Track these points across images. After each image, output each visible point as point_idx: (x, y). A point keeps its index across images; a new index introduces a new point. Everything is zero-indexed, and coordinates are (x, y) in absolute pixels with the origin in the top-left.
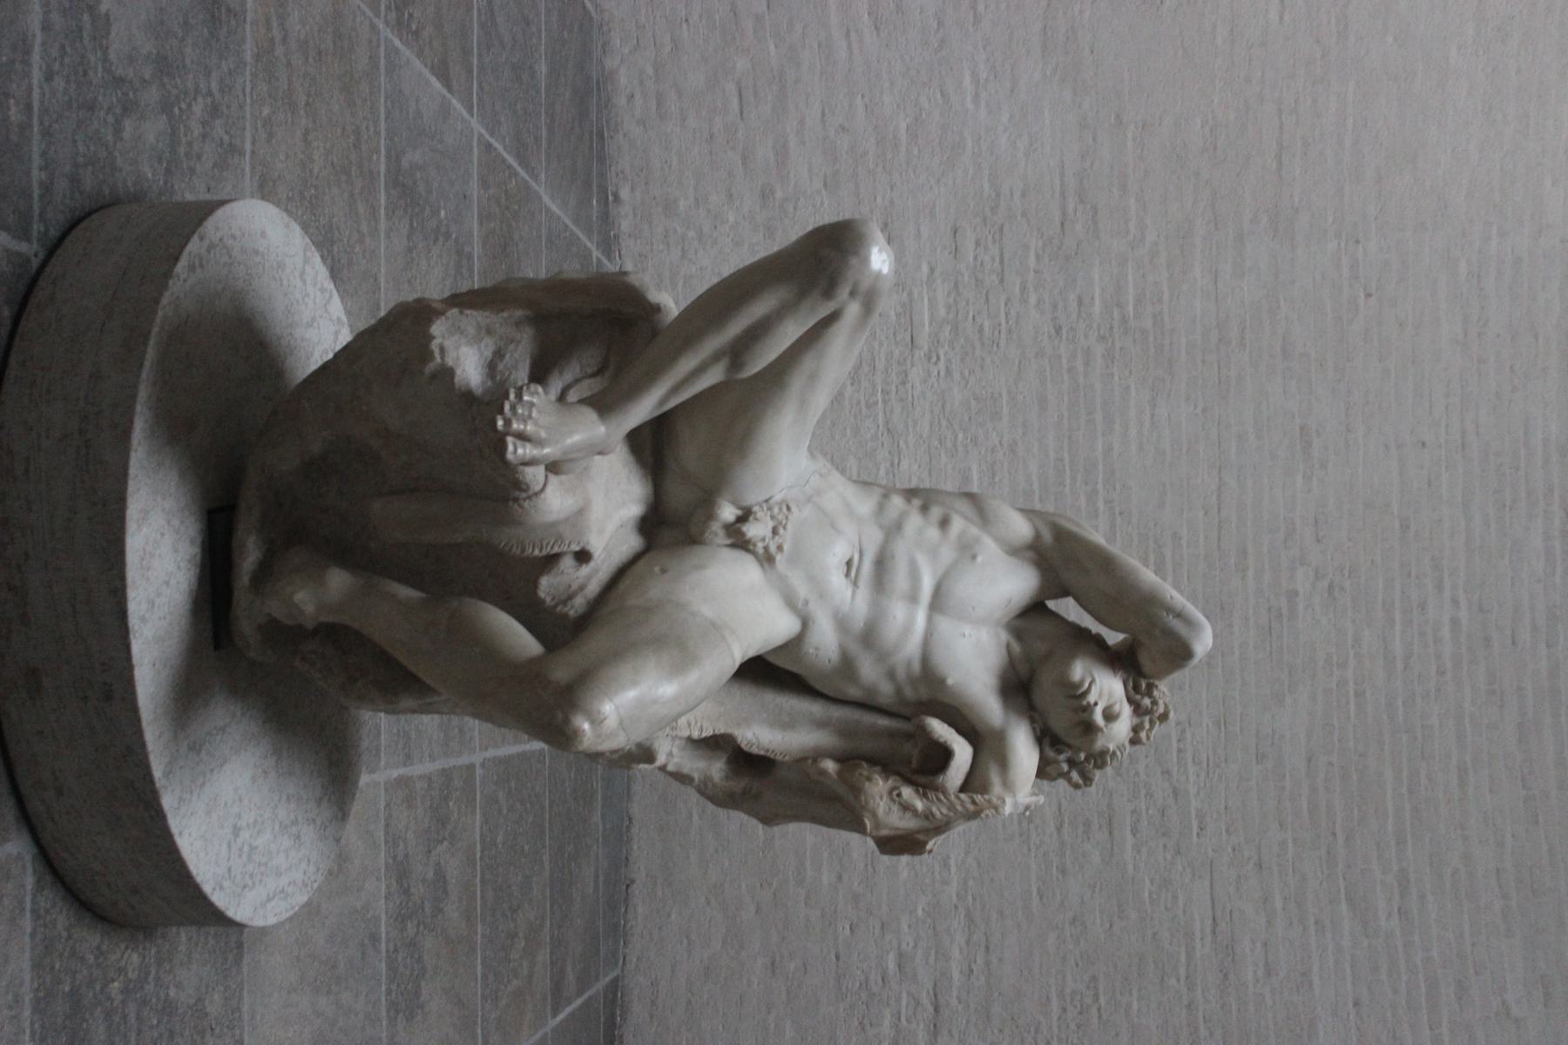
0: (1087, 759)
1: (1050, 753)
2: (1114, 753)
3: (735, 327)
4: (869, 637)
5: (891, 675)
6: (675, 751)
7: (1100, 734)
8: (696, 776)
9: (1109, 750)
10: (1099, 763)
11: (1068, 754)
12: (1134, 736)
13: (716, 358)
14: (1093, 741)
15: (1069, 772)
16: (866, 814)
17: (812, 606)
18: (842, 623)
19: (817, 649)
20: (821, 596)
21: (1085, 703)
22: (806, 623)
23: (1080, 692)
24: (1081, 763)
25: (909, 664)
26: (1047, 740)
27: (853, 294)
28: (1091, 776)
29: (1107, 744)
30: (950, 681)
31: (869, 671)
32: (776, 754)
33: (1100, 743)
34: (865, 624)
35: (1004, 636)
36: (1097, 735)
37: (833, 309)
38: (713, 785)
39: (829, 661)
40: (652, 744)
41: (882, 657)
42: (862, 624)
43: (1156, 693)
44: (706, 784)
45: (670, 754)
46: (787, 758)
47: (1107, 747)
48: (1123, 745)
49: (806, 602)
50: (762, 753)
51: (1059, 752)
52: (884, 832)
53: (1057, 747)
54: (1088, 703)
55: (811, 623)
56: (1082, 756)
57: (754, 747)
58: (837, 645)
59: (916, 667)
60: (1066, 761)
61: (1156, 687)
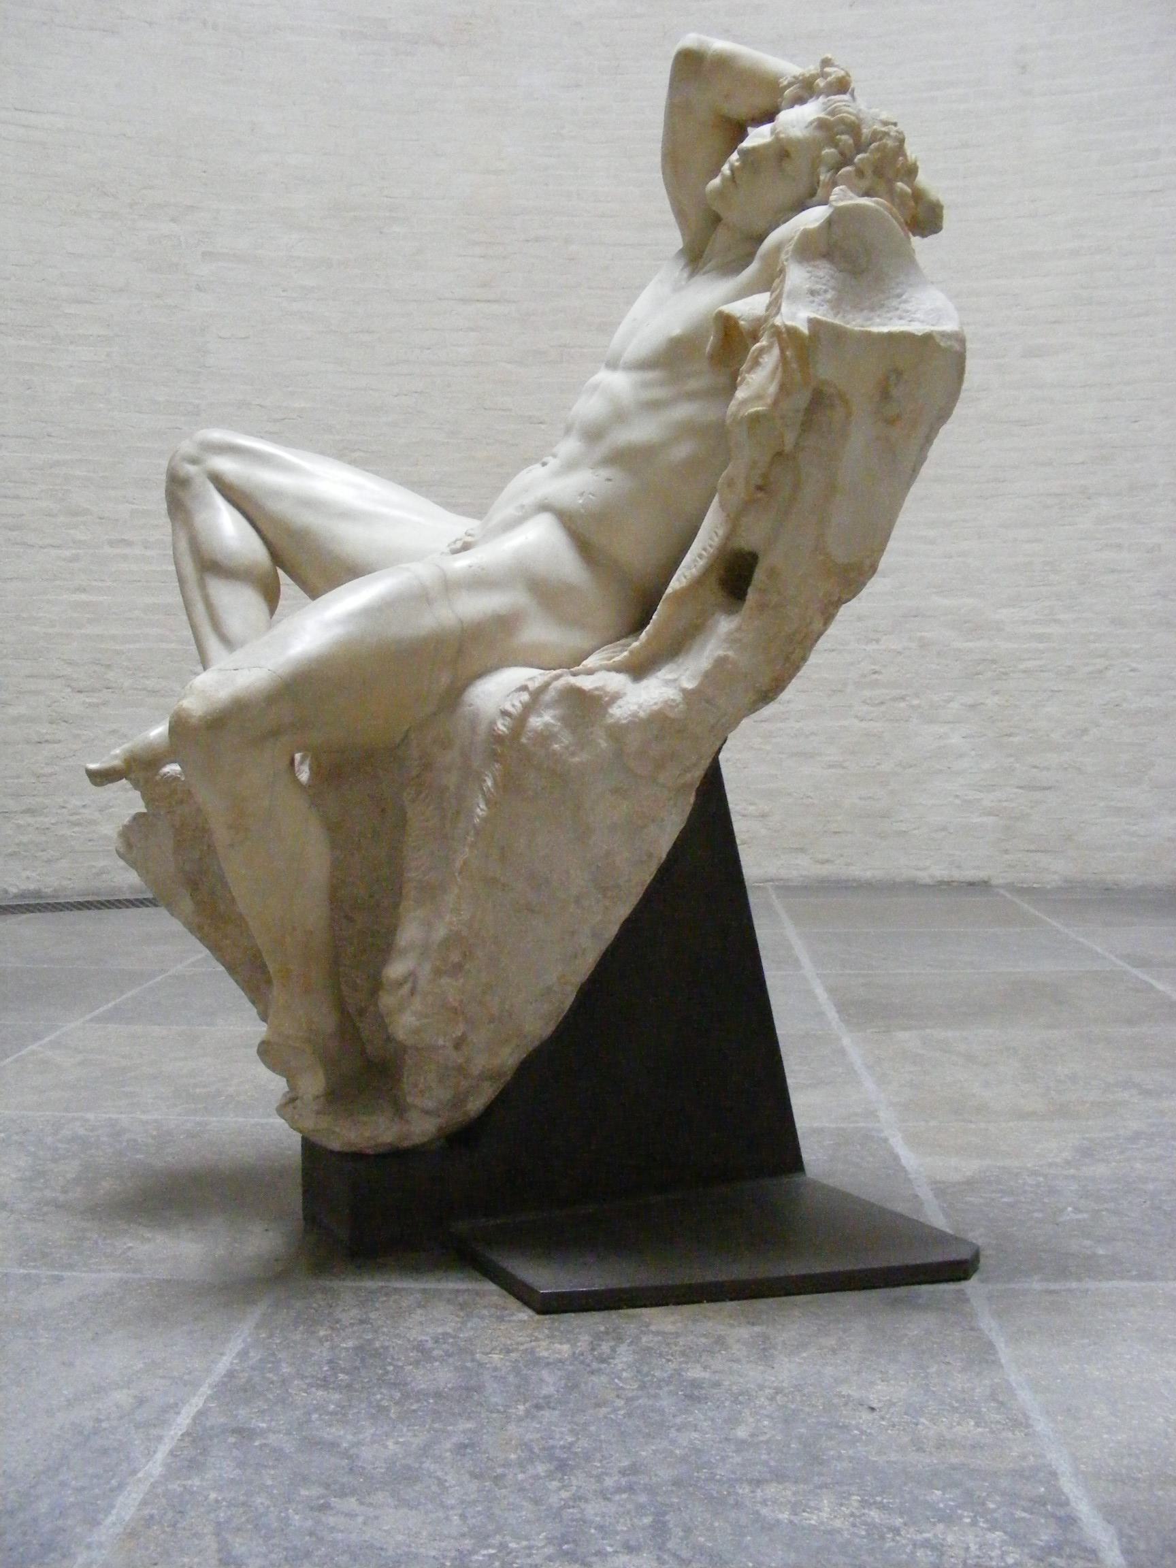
0: (836, 146)
2: (832, 113)
3: (189, 568)
4: (593, 434)
5: (654, 406)
6: (670, 677)
7: (782, 136)
8: (721, 653)
10: (843, 127)
11: (822, 169)
13: (203, 586)
16: (741, 414)
17: (529, 499)
18: (571, 466)
19: (582, 494)
20: (527, 491)
22: (544, 507)
24: (842, 154)
25: (645, 385)
27: (194, 461)
29: (806, 124)
30: (676, 331)
31: (642, 431)
32: (711, 546)
33: (797, 132)
34: (580, 441)
35: (700, 280)
37: (207, 480)
38: (739, 629)
39: (609, 480)
40: (555, 689)
41: (619, 416)
42: (578, 444)
43: (785, 83)
44: (735, 641)
45: (667, 683)
46: (721, 532)
47: (811, 123)
49: (522, 506)
50: (701, 563)
52: (773, 389)
54: (737, 160)
55: (546, 501)
56: (828, 151)
57: (686, 574)
58: (591, 471)
59: (650, 375)
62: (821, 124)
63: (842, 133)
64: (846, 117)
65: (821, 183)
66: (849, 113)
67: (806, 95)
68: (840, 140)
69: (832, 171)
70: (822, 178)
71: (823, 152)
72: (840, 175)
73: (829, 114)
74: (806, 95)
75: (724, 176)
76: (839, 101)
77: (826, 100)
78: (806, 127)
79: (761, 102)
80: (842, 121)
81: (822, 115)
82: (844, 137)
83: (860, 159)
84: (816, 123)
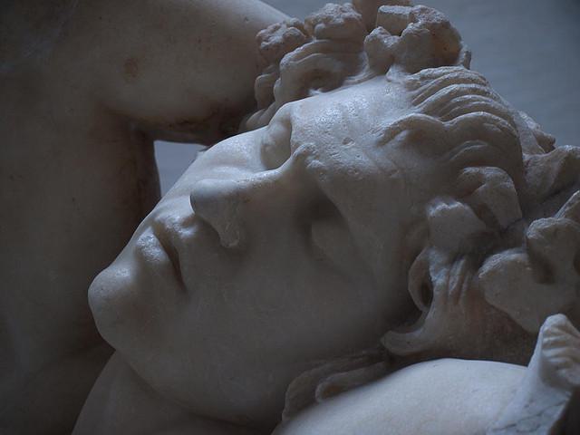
0: (465, 192)
1: (434, 321)
2: (444, 108)
7: (315, 163)
9: (408, 124)
11: (435, 257)
12: (399, 63)
14: (346, 179)
15: (530, 248)
21: (187, 233)
23: (156, 253)
24: (481, 211)
26: (395, 341)
28: (556, 166)
29: (375, 137)
33: (355, 156)
36: (319, 169)
43: (277, 38)
47: (392, 133)
48: (411, 86)
51: (427, 291)
53: (418, 303)
54: (187, 223)
60: (477, 263)
61: (260, 40)
62: (417, 137)
63: (480, 162)
64: (485, 119)
65: (436, 293)
66: (486, 108)
67: (336, 67)
68: (479, 180)
69: (458, 268)
70: (438, 280)
71: (433, 212)
72: (493, 272)
73: (425, 112)
74: (336, 67)
75: (143, 261)
76: (457, 81)
77: (410, 77)
78: (381, 143)
79: (213, 83)
80: (476, 131)
81: (414, 113)
82: (490, 172)
83: (543, 232)
84: (403, 134)
